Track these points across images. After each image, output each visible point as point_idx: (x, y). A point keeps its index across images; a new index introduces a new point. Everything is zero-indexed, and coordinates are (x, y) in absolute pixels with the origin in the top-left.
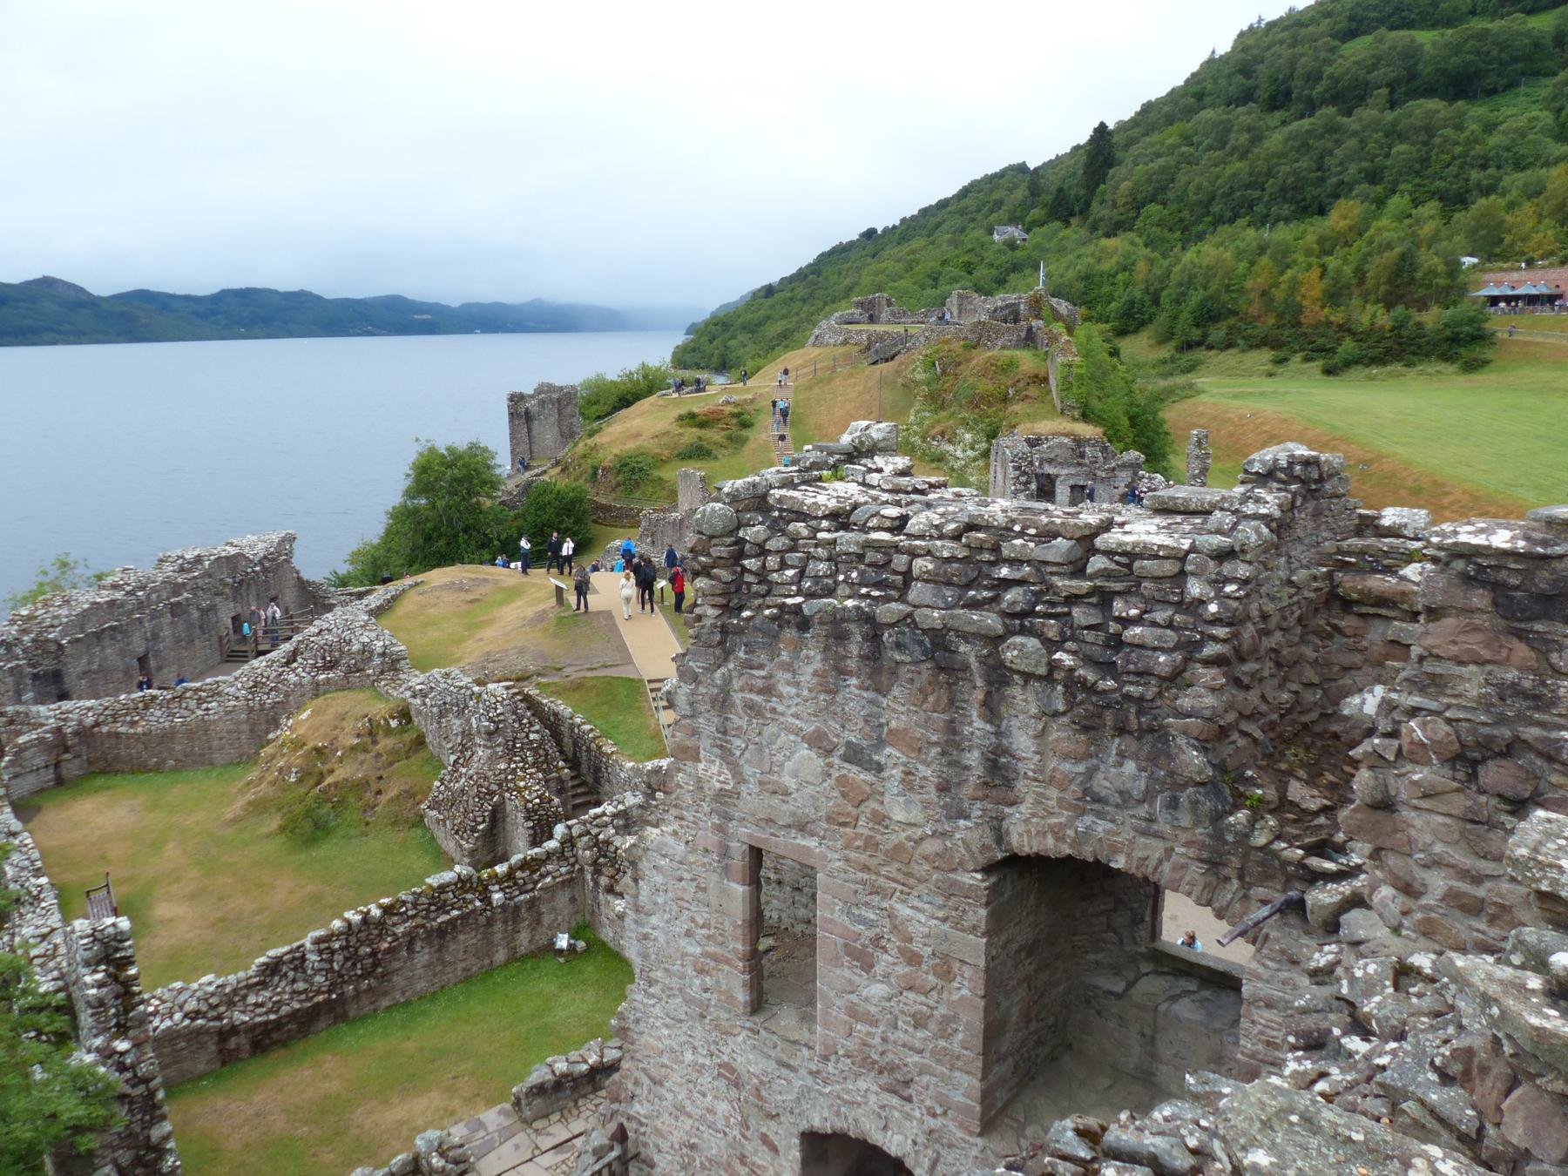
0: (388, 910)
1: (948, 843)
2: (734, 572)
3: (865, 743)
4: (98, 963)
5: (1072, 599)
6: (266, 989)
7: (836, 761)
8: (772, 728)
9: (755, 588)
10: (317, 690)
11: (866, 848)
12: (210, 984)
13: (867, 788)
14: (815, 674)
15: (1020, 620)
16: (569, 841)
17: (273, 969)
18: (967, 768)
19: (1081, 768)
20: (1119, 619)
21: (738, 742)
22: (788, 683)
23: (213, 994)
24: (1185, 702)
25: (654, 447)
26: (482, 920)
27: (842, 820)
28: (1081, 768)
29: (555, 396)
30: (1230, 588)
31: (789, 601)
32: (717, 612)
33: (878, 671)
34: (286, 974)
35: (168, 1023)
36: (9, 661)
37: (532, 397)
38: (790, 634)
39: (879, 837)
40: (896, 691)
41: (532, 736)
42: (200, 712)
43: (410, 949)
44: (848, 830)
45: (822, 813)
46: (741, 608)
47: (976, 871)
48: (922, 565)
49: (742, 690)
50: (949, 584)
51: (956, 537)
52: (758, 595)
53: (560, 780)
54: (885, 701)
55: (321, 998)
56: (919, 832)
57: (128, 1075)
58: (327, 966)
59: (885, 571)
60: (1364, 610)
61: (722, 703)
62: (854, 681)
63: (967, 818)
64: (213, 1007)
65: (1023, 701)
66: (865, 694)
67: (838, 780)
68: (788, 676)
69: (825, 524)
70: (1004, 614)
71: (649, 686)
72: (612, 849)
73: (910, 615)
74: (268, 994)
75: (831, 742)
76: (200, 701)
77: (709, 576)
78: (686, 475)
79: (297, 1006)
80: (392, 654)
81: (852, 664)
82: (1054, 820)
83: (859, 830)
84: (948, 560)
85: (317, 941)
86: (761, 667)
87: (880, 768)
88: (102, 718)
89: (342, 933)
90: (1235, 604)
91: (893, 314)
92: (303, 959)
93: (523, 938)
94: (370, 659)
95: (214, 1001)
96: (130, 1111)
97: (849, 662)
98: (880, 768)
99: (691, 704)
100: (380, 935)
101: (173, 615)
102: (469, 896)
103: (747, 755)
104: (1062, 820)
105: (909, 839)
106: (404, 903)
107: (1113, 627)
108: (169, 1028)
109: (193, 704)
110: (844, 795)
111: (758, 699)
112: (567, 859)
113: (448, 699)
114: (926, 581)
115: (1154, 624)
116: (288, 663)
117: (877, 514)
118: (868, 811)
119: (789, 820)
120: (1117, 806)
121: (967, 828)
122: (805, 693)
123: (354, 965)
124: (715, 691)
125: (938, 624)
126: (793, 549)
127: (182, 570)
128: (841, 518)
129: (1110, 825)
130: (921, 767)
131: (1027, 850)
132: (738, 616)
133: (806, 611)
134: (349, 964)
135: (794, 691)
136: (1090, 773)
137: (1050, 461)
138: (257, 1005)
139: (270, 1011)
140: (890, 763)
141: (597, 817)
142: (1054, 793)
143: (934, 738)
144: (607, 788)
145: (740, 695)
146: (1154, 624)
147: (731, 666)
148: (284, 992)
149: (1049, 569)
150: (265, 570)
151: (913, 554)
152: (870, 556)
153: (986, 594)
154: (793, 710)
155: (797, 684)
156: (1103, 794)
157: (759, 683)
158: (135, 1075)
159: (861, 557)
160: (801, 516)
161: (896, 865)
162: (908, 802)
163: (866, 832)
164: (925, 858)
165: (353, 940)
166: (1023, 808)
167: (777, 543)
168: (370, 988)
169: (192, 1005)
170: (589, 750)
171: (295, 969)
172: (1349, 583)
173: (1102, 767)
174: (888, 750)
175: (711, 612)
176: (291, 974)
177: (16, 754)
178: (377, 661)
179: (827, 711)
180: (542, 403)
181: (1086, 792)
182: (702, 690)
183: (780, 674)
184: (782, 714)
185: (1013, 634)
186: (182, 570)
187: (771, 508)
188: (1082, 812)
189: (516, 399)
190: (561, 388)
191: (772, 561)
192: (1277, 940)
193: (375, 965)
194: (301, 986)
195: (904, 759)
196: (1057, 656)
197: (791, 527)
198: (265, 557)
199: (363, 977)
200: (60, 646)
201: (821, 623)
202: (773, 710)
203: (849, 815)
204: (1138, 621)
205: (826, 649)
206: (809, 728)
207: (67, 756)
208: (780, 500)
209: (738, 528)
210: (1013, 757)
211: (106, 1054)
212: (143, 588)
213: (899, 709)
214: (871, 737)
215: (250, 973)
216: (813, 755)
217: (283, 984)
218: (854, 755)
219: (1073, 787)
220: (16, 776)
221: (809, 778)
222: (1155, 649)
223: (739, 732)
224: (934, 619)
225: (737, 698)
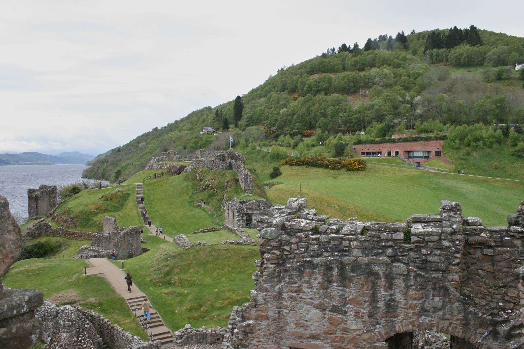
1: (372, 334)
2: (280, 251)
3: (339, 305)
5: (410, 250)
7: (327, 312)
8: (302, 304)
9: (289, 256)
11: (340, 340)
13: (340, 320)
14: (319, 283)
15: (394, 258)
18: (379, 308)
19: (420, 302)
20: (424, 255)
21: (285, 311)
22: (308, 288)
24: (450, 278)
25: (92, 208)
27: (330, 332)
28: (420, 302)
29: (47, 190)
30: (457, 242)
31: (308, 259)
32: (274, 266)
33: (344, 280)
37: (37, 190)
38: (308, 270)
39: (345, 336)
40: (352, 285)
41: (86, 326)
44: (332, 336)
45: (322, 331)
46: (283, 264)
47: (383, 341)
48: (354, 244)
49: (287, 292)
50: (365, 248)
51: (362, 233)
52: (291, 258)
53: (99, 343)
54: (347, 290)
56: (361, 332)
59: (339, 247)
60: (476, 246)
61: (279, 296)
62: (335, 284)
63: (379, 324)
65: (400, 282)
66: (339, 288)
67: (328, 319)
68: (307, 285)
69: (310, 233)
70: (389, 257)
71: (128, 302)
73: (356, 260)
75: (325, 306)
77: (269, 253)
78: (108, 219)
81: (334, 278)
82: (411, 320)
83: (337, 335)
84: (365, 241)
86: (296, 283)
87: (346, 312)
90: (459, 247)
91: (177, 158)
97: (333, 278)
98: (346, 312)
99: (264, 299)
103: (290, 315)
104: (414, 319)
105: (357, 335)
107: (424, 258)
110: (331, 324)
111: (295, 295)
113: (46, 314)
114: (358, 249)
115: (436, 255)
117: (329, 228)
118: (341, 328)
119: (308, 336)
120: (433, 312)
121: (380, 327)
122: (315, 290)
124: (276, 294)
125: (367, 262)
126: (300, 242)
128: (315, 231)
129: (430, 319)
130: (362, 310)
131: (402, 331)
132: (284, 266)
133: (315, 263)
135: (309, 290)
136: (424, 303)
137: (250, 209)
140: (349, 310)
142: (411, 311)
143: (367, 299)
144: (116, 344)
145: (287, 294)
146: (436, 255)
147: (283, 284)
149: (398, 242)
151: (350, 240)
152: (333, 242)
153: (380, 251)
154: (310, 296)
155: (311, 288)
156: (428, 309)
157: (295, 289)
159: (329, 243)
160: (301, 231)
161: (352, 344)
162: (357, 322)
163: (340, 335)
164: (364, 340)
166: (400, 318)
167: (294, 240)
170: (108, 329)
172: (471, 239)
173: (427, 300)
174: (348, 306)
175: (271, 266)
179: (326, 295)
180: (42, 193)
181: (422, 309)
182: (269, 294)
183: (304, 285)
184: (305, 299)
185: (393, 262)
187: (287, 228)
188: (420, 316)
189: (31, 191)
190: (50, 187)
191: (294, 247)
192: (486, 344)
195: (355, 308)
196: (411, 267)
197: (299, 234)
201: (321, 266)
202: (301, 298)
203: (333, 330)
204: (430, 254)
205: (324, 274)
206: (316, 302)
208: (290, 225)
209: (278, 237)
210: (396, 301)
213: (352, 292)
214: (342, 303)
216: (318, 311)
218: (335, 309)
219: (417, 308)
221: (317, 320)
222: (438, 263)
223: (286, 307)
224: (366, 261)
225: (285, 295)
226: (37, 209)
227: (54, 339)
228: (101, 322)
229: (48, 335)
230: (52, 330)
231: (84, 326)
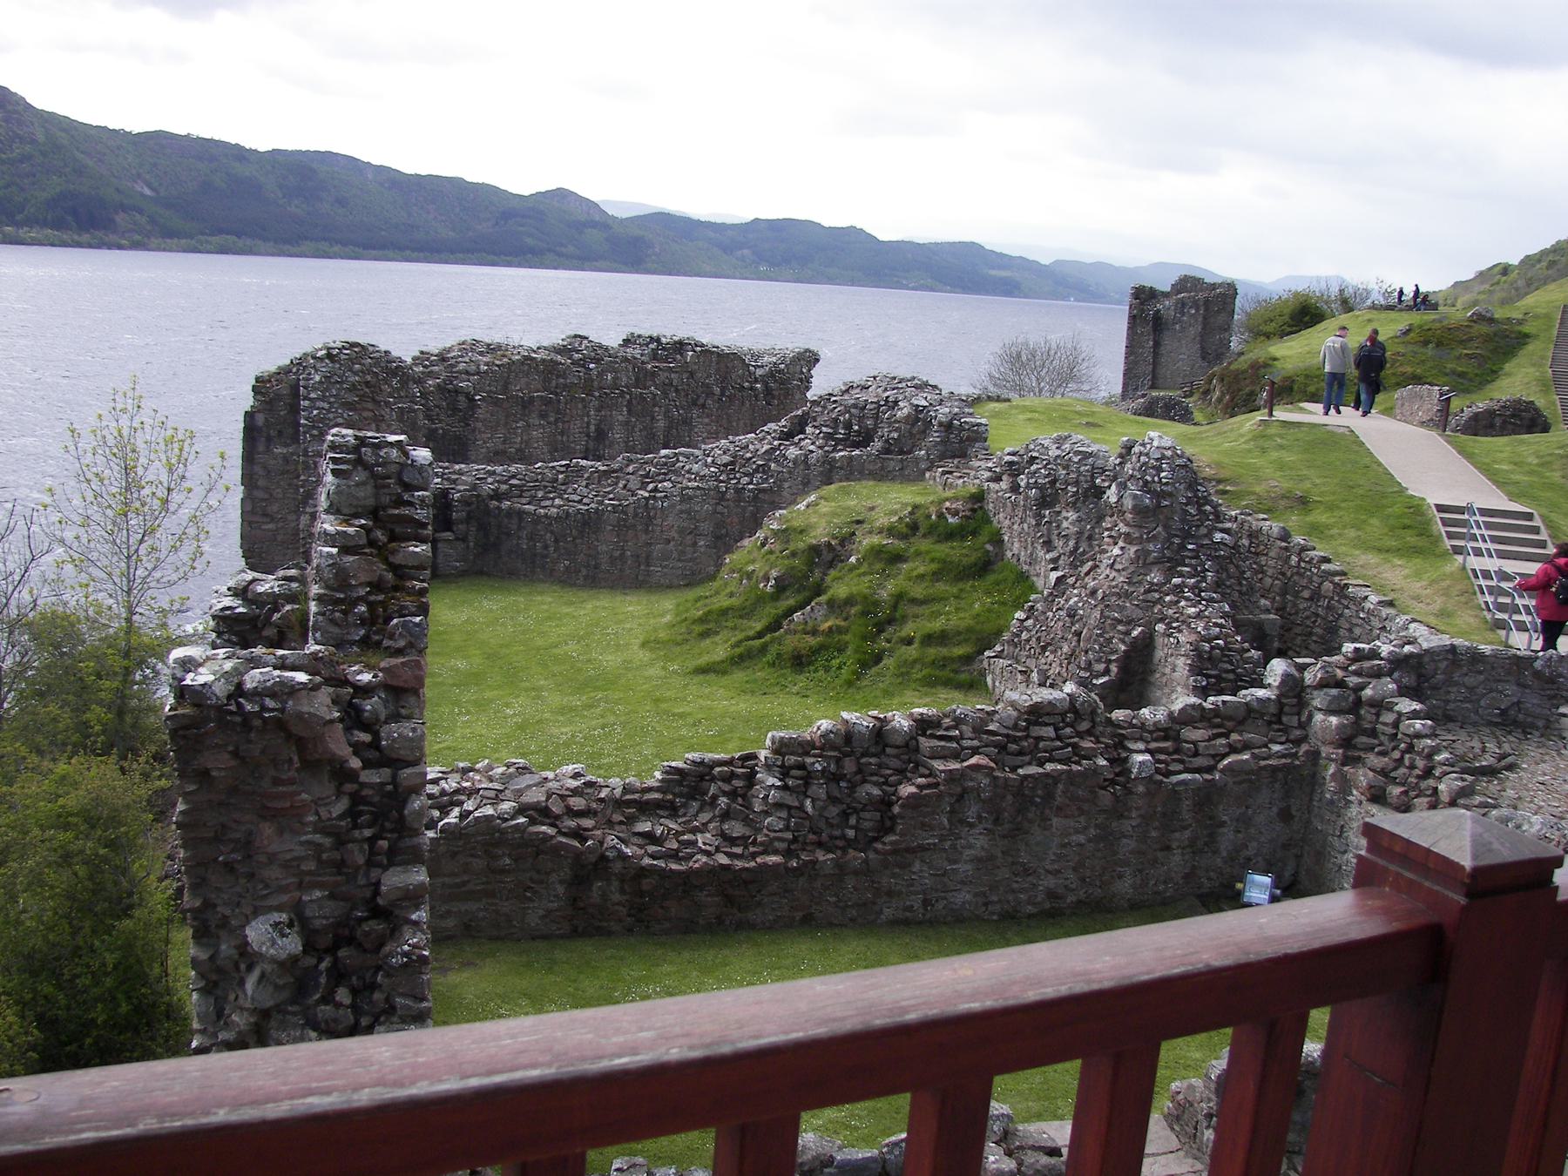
0: (924, 725)
4: (357, 516)
10: (829, 473)
12: (576, 776)
16: (1294, 688)
17: (690, 784)
23: (575, 792)
26: (1105, 798)
34: (715, 798)
35: (489, 811)
37: (1166, 295)
41: (1218, 536)
43: (957, 819)
55: (773, 859)
57: (365, 737)
58: (791, 800)
72: (1388, 718)
79: (723, 860)
80: (961, 428)
85: (781, 748)
88: (504, 487)
89: (834, 748)
92: (751, 778)
93: (1177, 861)
94: (924, 432)
95: (577, 803)
96: (352, 813)
100: (901, 772)
101: (629, 411)
102: (1087, 744)
106: (959, 722)
108: (488, 818)
112: (1286, 730)
116: (787, 436)
123: (845, 815)
127: (654, 356)
134: (834, 811)
138: (650, 837)
139: (674, 855)
141: (1359, 656)
148: (703, 828)
150: (768, 391)
158: (375, 744)
168: (866, 871)
169: (535, 796)
170: (1316, 596)
171: (733, 795)
176: (723, 801)
178: (934, 437)
190: (1214, 286)
193: (886, 826)
194: (736, 829)
198: (771, 374)
199: (850, 844)
200: (472, 400)
207: (448, 535)
211: (328, 674)
212: (597, 361)
215: (652, 783)
217: (704, 817)
226: (1155, 364)
227: (1071, 580)
229: (1055, 560)
231: (1209, 535)
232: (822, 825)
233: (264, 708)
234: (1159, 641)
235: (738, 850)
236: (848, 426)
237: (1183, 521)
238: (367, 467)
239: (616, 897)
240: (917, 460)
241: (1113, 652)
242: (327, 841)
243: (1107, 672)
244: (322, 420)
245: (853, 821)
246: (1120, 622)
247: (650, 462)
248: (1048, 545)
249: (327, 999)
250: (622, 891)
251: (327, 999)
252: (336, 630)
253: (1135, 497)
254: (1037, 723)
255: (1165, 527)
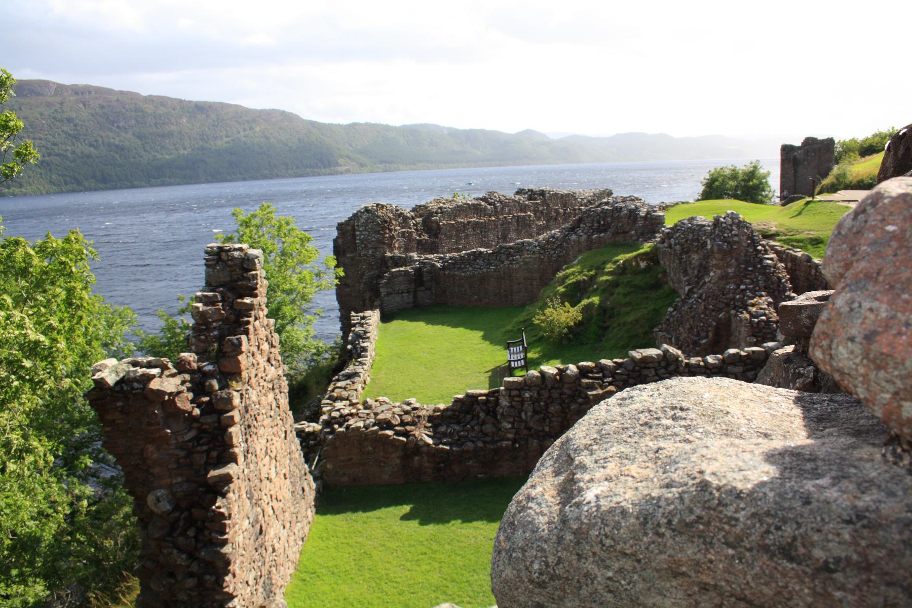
6: (458, 423)
34: (478, 413)
36: (403, 227)
37: (799, 148)
42: (506, 262)
64: (403, 423)
74: (457, 427)
76: (509, 255)
89: (537, 386)
92: (497, 403)
95: (408, 418)
109: (504, 257)
165: (545, 394)
171: (487, 413)
176: (482, 415)
177: (389, 279)
178: (640, 223)
180: (807, 153)
186: (530, 199)
189: (787, 151)
194: (488, 428)
217: (473, 423)
220: (389, 294)
228: (813, 271)
230: (696, 272)
232: (531, 424)
233: (133, 389)
234: (733, 319)
235: (488, 439)
236: (599, 222)
237: (745, 256)
238: (224, 262)
239: (426, 464)
240: (632, 236)
241: (710, 326)
242: (182, 453)
243: (707, 337)
244: (366, 240)
245: (547, 421)
246: (713, 311)
247: (511, 248)
248: (685, 273)
249: (184, 533)
250: (429, 462)
251: (184, 533)
252: (202, 345)
253: (719, 245)
254: (645, 368)
255: (737, 260)
